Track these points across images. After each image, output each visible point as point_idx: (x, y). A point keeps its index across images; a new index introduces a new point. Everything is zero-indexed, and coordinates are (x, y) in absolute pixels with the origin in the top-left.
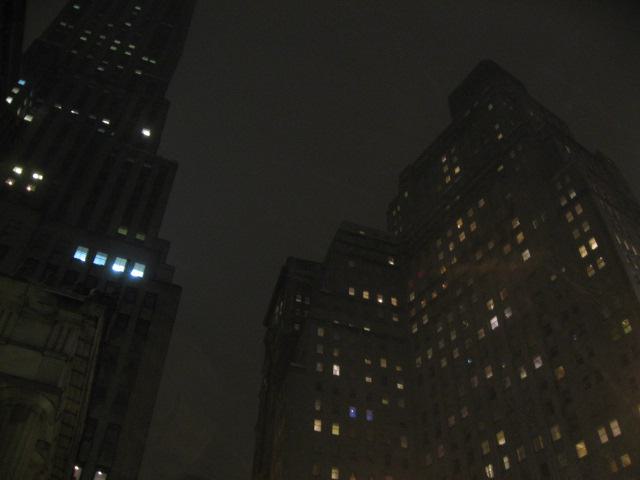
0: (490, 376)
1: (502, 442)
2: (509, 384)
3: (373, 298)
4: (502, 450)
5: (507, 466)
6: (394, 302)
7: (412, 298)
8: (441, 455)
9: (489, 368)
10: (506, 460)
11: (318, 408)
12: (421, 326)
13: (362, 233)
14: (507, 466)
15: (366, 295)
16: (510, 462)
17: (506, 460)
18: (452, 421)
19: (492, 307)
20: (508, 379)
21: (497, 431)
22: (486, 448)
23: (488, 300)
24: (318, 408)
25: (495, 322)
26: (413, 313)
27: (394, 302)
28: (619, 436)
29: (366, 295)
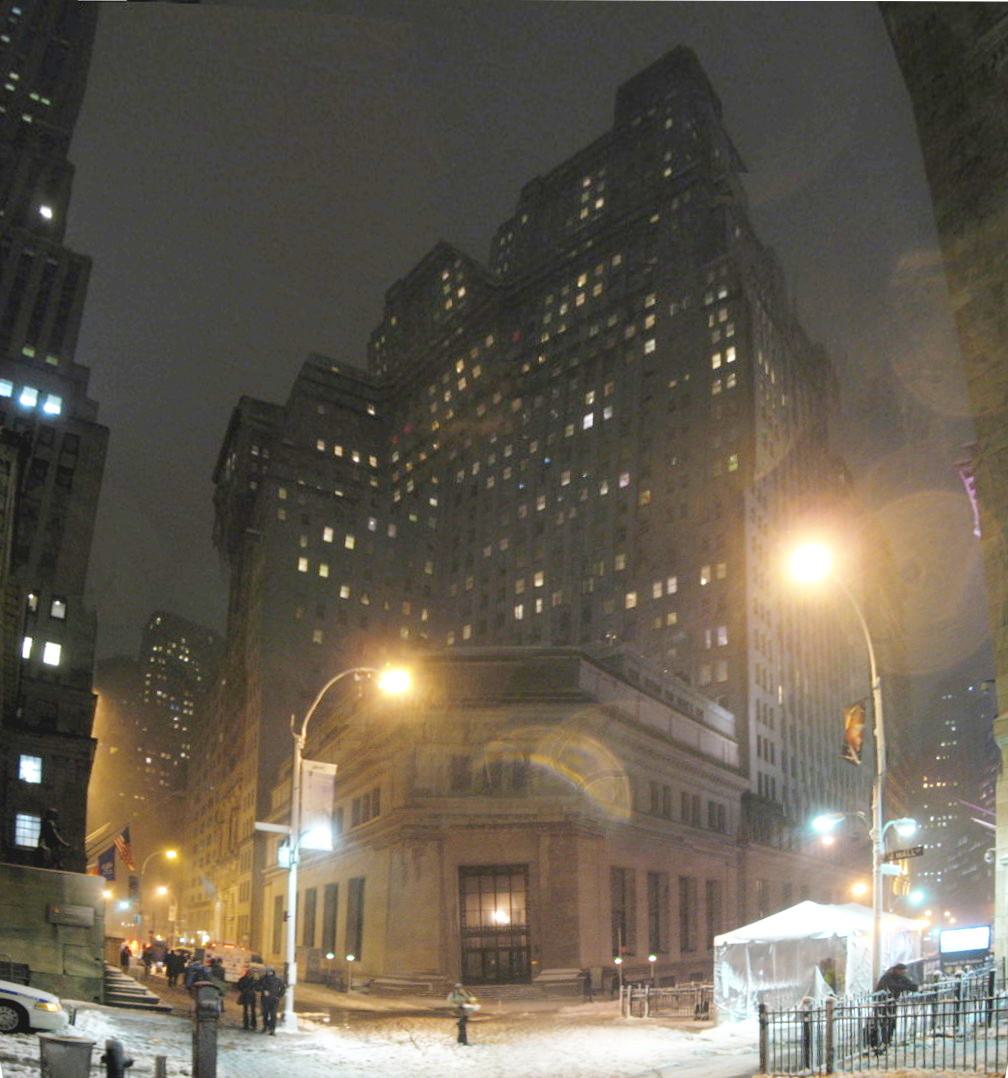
0: (541, 507)
1: (539, 583)
2: (584, 498)
3: (347, 455)
4: (538, 593)
5: (539, 609)
6: (373, 461)
7: (396, 458)
8: (469, 587)
9: (542, 499)
10: (539, 603)
11: (304, 544)
12: (404, 494)
13: (335, 369)
14: (539, 609)
15: (338, 451)
16: (543, 606)
17: (539, 603)
18: (488, 552)
19: (591, 401)
20: (585, 491)
21: (536, 571)
22: (520, 587)
23: (590, 391)
24: (304, 544)
25: (589, 421)
26: (396, 477)
27: (373, 461)
28: (659, 599)
29: (338, 451)
